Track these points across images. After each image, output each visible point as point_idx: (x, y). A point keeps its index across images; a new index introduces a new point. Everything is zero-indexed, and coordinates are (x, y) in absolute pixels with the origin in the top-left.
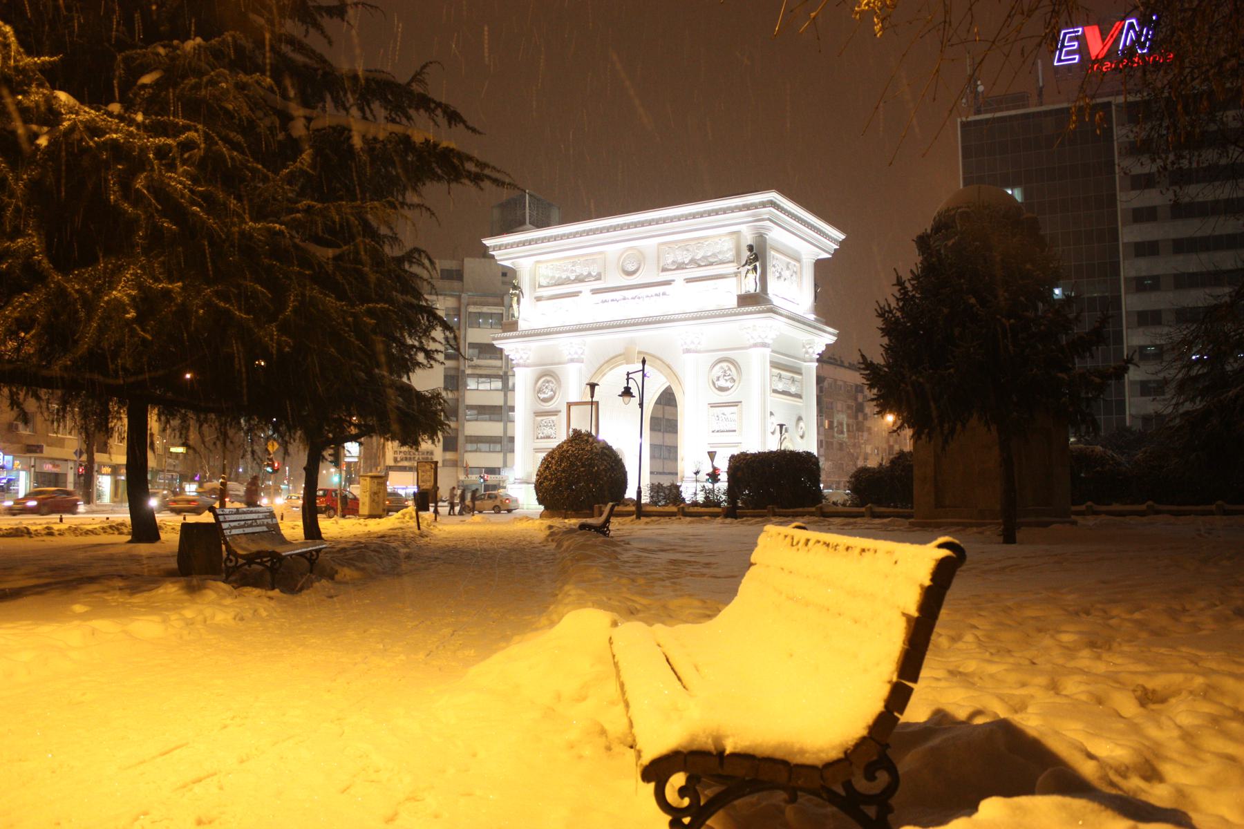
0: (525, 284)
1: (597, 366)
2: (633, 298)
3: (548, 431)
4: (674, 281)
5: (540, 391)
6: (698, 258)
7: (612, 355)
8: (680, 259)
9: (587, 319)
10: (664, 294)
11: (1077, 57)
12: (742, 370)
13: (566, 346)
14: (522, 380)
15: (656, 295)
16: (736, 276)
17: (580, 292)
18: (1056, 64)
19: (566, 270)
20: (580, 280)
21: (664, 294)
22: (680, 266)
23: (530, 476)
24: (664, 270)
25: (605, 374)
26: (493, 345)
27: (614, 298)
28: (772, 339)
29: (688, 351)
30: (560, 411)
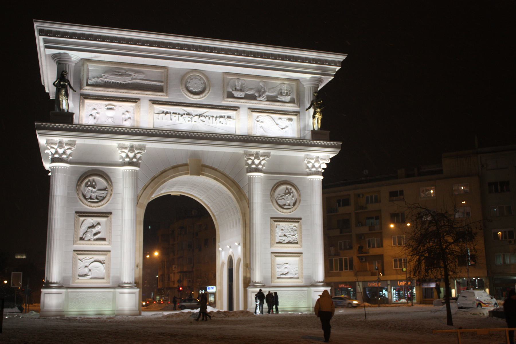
1: (156, 174)
2: (197, 115)
4: (239, 108)
7: (174, 164)
10: (229, 117)
12: (301, 192)
15: (221, 117)
16: (296, 115)
17: (139, 99)
21: (229, 117)
23: (65, 279)
24: (230, 96)
25: (165, 182)
27: (177, 112)
28: (323, 169)
30: (111, 213)
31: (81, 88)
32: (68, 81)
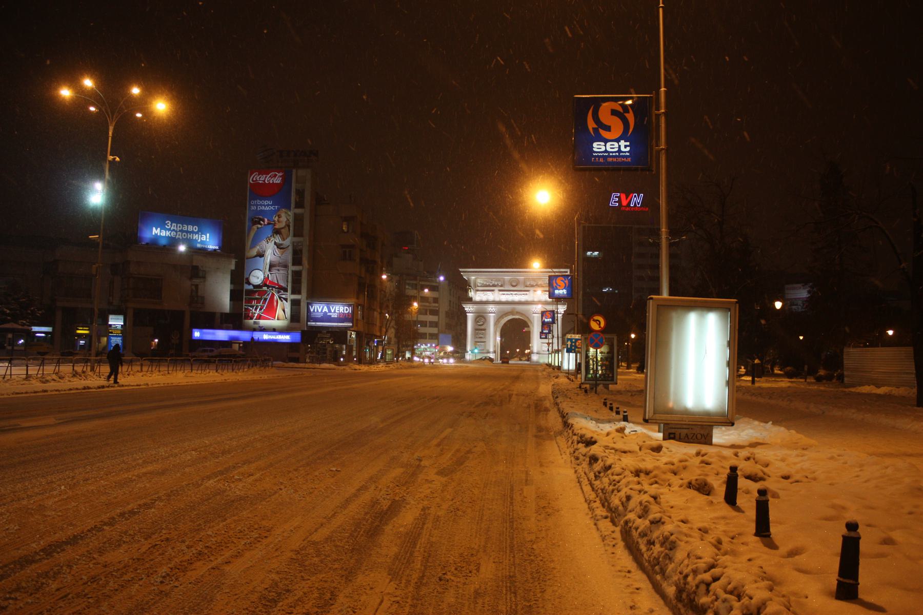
0: (472, 285)
3: (481, 336)
5: (478, 322)
6: (539, 284)
8: (532, 283)
9: (497, 299)
11: (617, 204)
13: (491, 308)
14: (470, 317)
18: (610, 205)
19: (488, 282)
20: (494, 286)
22: (532, 286)
24: (526, 286)
26: (462, 306)
29: (534, 313)
31: (475, 287)
32: (471, 286)
